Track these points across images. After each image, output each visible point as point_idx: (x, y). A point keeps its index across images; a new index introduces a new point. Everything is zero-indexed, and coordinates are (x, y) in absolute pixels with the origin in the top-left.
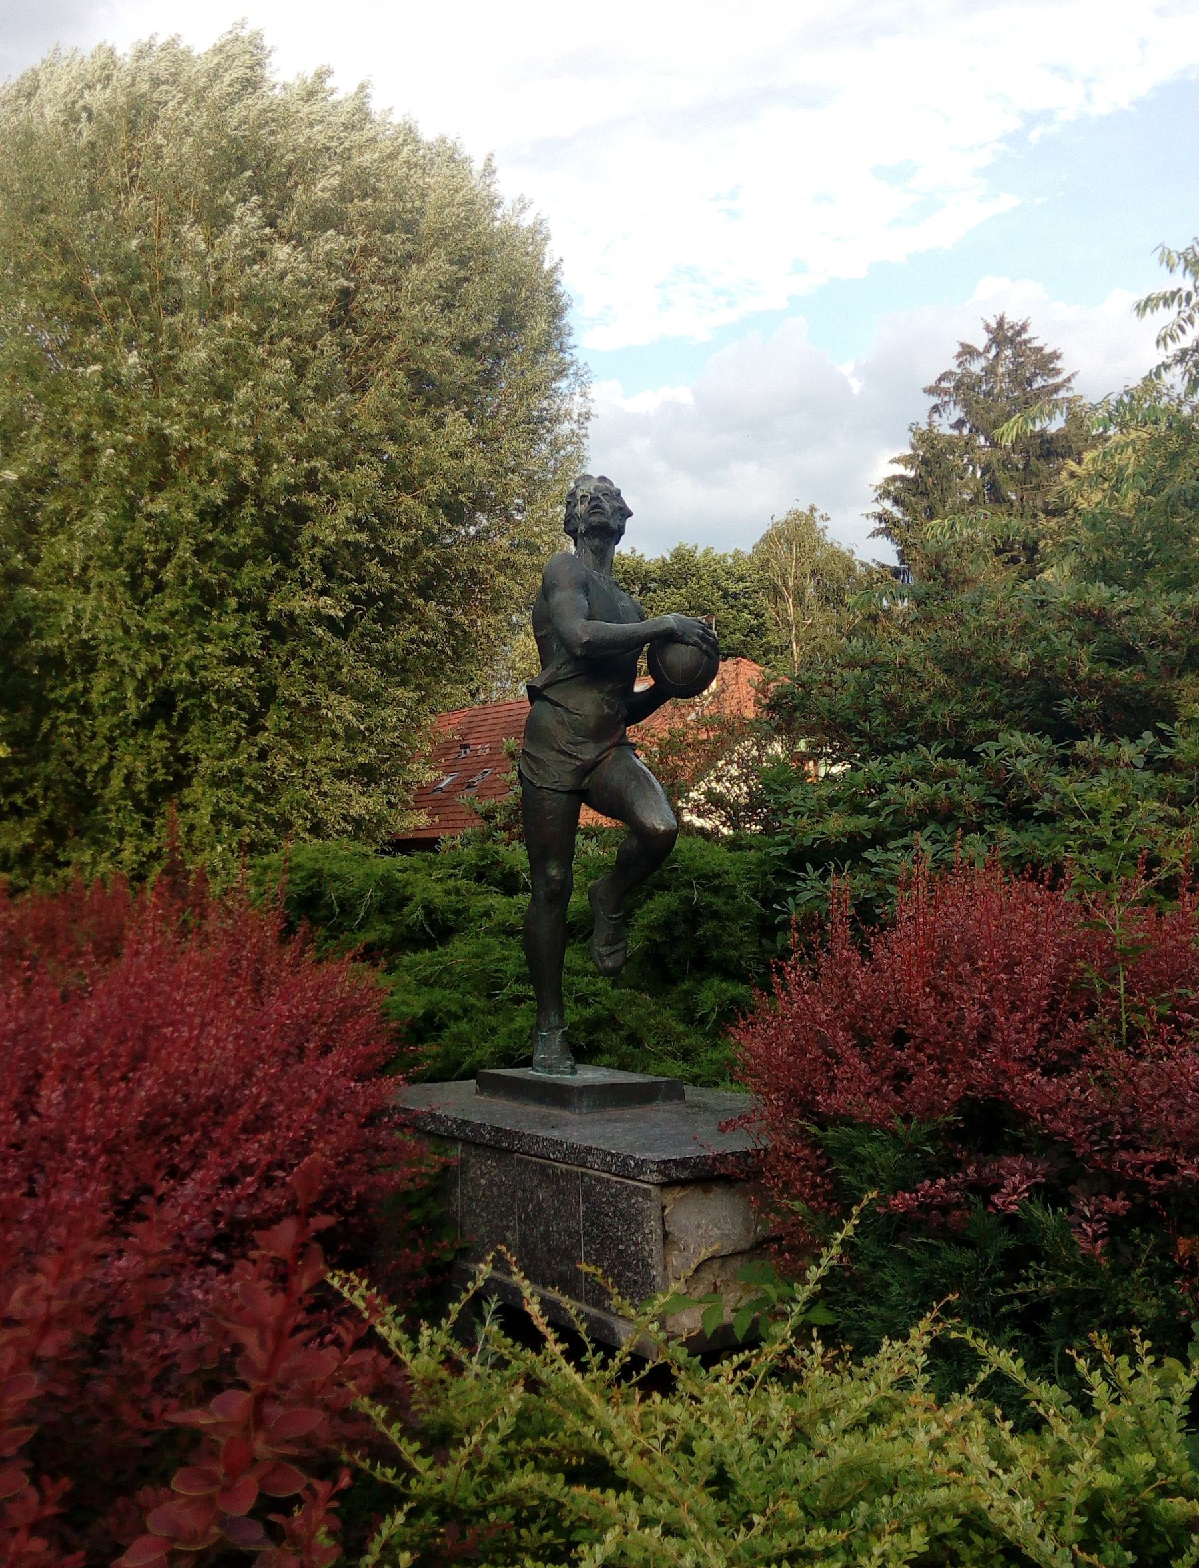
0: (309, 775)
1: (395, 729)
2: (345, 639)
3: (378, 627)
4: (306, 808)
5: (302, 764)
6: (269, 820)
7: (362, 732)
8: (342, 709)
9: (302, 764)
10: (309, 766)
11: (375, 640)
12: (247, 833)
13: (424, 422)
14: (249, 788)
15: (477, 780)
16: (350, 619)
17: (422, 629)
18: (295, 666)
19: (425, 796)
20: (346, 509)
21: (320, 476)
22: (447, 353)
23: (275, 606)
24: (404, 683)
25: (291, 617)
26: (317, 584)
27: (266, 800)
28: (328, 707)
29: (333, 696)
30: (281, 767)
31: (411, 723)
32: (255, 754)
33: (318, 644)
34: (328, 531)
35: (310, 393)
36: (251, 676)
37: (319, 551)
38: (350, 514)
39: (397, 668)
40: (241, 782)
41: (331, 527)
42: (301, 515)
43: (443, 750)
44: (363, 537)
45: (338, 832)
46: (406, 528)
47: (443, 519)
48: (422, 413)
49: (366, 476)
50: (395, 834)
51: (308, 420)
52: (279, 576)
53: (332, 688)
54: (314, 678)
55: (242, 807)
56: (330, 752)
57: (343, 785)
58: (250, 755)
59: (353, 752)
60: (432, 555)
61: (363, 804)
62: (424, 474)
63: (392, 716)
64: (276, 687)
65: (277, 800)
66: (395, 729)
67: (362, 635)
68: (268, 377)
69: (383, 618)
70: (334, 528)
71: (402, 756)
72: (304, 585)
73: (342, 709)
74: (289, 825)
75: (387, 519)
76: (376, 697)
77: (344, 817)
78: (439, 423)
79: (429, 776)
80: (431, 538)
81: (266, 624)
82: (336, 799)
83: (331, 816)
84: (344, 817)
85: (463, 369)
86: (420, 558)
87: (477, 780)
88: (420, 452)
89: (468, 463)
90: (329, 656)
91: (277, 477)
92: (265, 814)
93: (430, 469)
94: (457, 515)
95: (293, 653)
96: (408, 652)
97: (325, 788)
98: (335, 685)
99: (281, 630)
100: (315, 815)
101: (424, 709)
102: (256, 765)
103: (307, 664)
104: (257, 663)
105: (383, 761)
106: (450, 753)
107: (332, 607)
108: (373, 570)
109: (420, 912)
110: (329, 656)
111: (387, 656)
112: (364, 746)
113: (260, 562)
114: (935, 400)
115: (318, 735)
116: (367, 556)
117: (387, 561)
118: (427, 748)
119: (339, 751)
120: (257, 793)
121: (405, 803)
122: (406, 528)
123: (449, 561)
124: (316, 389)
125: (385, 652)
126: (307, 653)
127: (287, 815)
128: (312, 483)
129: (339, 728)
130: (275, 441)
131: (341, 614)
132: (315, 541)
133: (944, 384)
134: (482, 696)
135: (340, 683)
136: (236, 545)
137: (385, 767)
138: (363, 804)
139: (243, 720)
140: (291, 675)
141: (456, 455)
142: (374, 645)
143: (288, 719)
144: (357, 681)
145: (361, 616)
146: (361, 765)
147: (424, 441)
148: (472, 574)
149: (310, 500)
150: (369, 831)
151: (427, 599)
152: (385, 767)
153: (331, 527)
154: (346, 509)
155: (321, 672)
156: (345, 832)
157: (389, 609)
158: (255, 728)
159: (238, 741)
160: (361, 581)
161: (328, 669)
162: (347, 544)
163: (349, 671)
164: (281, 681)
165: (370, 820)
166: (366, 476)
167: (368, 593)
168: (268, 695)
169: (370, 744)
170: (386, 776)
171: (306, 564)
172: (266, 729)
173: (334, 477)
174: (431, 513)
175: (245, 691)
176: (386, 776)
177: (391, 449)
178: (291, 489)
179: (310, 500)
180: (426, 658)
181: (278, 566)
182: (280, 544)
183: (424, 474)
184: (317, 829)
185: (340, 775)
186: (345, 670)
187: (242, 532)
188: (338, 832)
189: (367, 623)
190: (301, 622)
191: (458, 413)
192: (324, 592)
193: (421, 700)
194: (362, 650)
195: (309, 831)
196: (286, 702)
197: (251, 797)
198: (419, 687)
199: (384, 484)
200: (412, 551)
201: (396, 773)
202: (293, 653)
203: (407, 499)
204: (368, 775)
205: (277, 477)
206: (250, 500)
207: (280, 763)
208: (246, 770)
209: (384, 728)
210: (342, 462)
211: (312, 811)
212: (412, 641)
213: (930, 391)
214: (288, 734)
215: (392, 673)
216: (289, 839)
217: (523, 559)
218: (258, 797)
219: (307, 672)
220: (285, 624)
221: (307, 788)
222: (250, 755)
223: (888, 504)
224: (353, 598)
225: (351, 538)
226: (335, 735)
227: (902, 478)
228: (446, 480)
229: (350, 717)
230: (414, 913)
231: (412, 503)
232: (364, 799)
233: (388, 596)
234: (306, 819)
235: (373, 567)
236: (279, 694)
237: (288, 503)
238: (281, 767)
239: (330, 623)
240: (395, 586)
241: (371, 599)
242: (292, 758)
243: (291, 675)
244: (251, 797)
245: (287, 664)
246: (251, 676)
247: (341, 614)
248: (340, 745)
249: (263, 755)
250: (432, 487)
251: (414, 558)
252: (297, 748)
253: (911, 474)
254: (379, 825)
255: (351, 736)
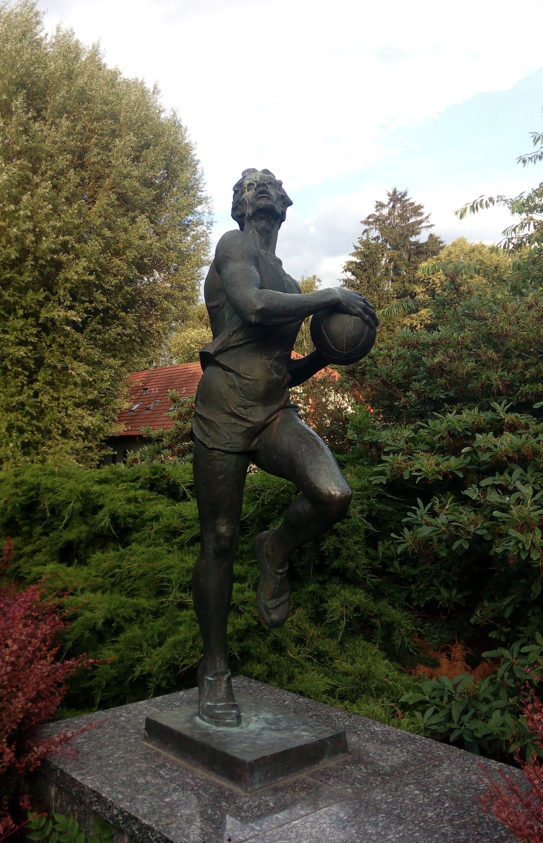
0: (61, 405)
1: (108, 380)
2: (82, 334)
3: (100, 327)
4: (59, 423)
5: (58, 399)
6: (38, 429)
7: (90, 382)
8: (80, 370)
9: (58, 399)
10: (61, 400)
11: (99, 334)
12: (27, 437)
13: (125, 219)
14: (28, 413)
15: (151, 406)
16: (85, 322)
17: (124, 328)
18: (54, 347)
19: (124, 416)
20: (83, 263)
21: (69, 246)
22: (137, 184)
23: (44, 315)
24: (114, 356)
25: (53, 321)
26: (68, 303)
27: (38, 419)
28: (72, 369)
29: (75, 363)
30: (46, 401)
31: (117, 378)
32: (31, 394)
33: (67, 335)
34: (73, 274)
35: (64, 200)
36: (31, 351)
37: (68, 285)
38: (85, 264)
39: (110, 348)
40: (23, 409)
41: (76, 271)
42: (59, 266)
43: (134, 391)
44: (92, 278)
45: (76, 435)
46: (115, 276)
47: (136, 271)
48: (124, 215)
49: (94, 245)
50: (108, 437)
51: (63, 216)
52: (47, 299)
53: (75, 359)
54: (65, 354)
55: (24, 422)
56: (73, 393)
57: (80, 411)
58: (29, 395)
59: (85, 393)
60: (129, 289)
61: (90, 420)
62: (125, 248)
63: (107, 374)
64: (44, 358)
65: (43, 419)
66: (108, 380)
67: (91, 331)
68: (40, 191)
69: (104, 322)
70: (76, 272)
71: (112, 395)
72: (60, 304)
73: (80, 370)
74: (50, 432)
75: (106, 271)
76: (99, 363)
77: (80, 428)
78: (133, 221)
79: (126, 405)
80: (130, 281)
81: (38, 325)
82: (76, 418)
83: (73, 428)
84: (80, 428)
85: (147, 194)
86: (123, 292)
87: (151, 406)
88: (123, 236)
89: (148, 242)
90: (73, 342)
91: (45, 244)
92: (36, 426)
93: (129, 245)
94: (144, 269)
95: (54, 340)
96: (116, 340)
97: (70, 412)
98: (76, 357)
99: (48, 327)
100: (63, 426)
101: (124, 369)
102: (32, 400)
103: (61, 346)
104: (32, 343)
105: (102, 397)
106: (137, 393)
107: (75, 316)
108: (97, 296)
109: (107, 521)
110: (73, 342)
111: (105, 343)
112: (91, 390)
113: (36, 291)
114: (367, 227)
115: (67, 384)
116: (95, 290)
117: (105, 292)
118: (126, 390)
119: (78, 392)
120: (31, 415)
121: (114, 421)
122: (115, 276)
123: (140, 293)
124: (66, 198)
125: (103, 340)
126: (61, 340)
127: (49, 427)
128: (65, 247)
129: (78, 380)
130: (45, 225)
131: (80, 320)
132: (67, 280)
133: (370, 220)
134: (154, 364)
135: (79, 357)
136: (23, 281)
137: (103, 400)
138: (90, 420)
139: (25, 376)
140: (52, 351)
141: (142, 238)
142: (98, 336)
143: (50, 375)
144: (88, 355)
145: (91, 321)
146: (90, 400)
147: (125, 230)
148: (151, 300)
149: (63, 257)
150: (93, 434)
151: (127, 313)
152: (103, 400)
153: (76, 271)
154: (83, 263)
155: (68, 350)
156: (80, 435)
157: (107, 317)
158: (31, 381)
159: (22, 387)
160: (91, 302)
161: (73, 349)
162: (83, 282)
163: (84, 350)
164: (47, 355)
165: (94, 429)
166: (94, 245)
167: (95, 308)
168: (40, 362)
169: (95, 389)
170: (102, 405)
171: (61, 292)
172: (37, 381)
173: (77, 246)
174: (129, 267)
175: (27, 360)
176: (102, 405)
177: (107, 233)
178: (54, 252)
179: (63, 257)
180: (124, 343)
181: (46, 293)
182: (48, 283)
183: (125, 248)
184: (65, 434)
185: (77, 405)
186: (82, 349)
187: (27, 274)
188: (76, 435)
189: (94, 324)
190: (58, 324)
191: (143, 216)
192: (71, 308)
193: (123, 365)
194: (91, 339)
195: (61, 435)
196: (49, 366)
197: (29, 418)
198: (122, 358)
199: (103, 252)
200: (119, 288)
201: (108, 404)
202: (54, 340)
203: (117, 261)
204: (93, 405)
205: (45, 244)
206: (30, 257)
207: (46, 399)
208: (26, 403)
209: (102, 380)
210: (80, 240)
211: (62, 425)
212: (118, 334)
213: (366, 223)
214: (50, 383)
215: (109, 351)
216: (50, 439)
217: (177, 293)
218: (33, 418)
219: (61, 350)
220: (49, 324)
221: (60, 412)
222: (29, 395)
223: (349, 275)
224: (87, 311)
225: (86, 278)
226: (76, 384)
227: (356, 263)
228: (137, 251)
229: (84, 374)
230: (103, 519)
231: (119, 262)
232: (90, 418)
233: (106, 310)
234: (59, 429)
235: (98, 295)
236: (45, 362)
237: (52, 258)
238: (46, 401)
239: (74, 324)
240: (110, 305)
241: (97, 311)
242: (52, 396)
243: (52, 351)
244: (29, 418)
245: (50, 346)
246: (31, 351)
247: (80, 320)
248: (78, 389)
249: (36, 395)
250: (130, 254)
251: (120, 291)
252: (55, 390)
253: (358, 261)
254: (99, 431)
255: (85, 384)
